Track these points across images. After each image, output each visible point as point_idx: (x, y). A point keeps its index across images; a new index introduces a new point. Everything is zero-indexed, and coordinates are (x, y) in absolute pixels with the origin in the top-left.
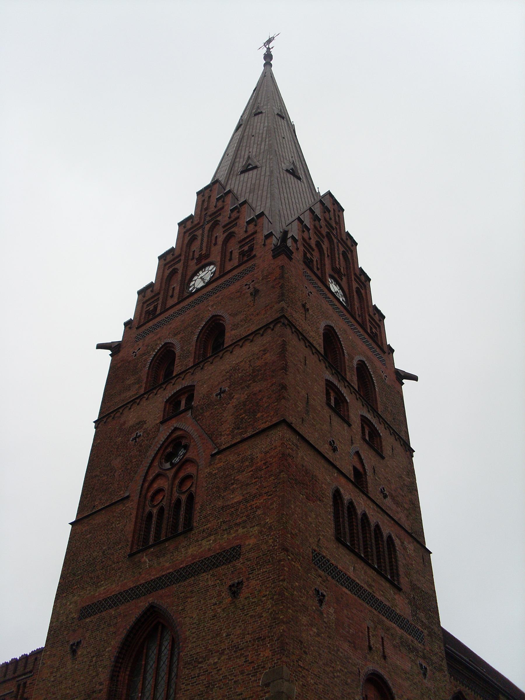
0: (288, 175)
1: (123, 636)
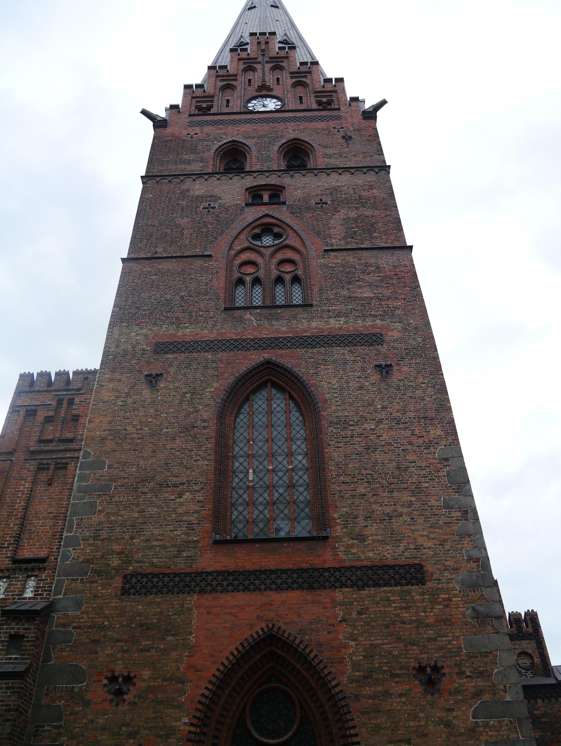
1: (231, 381)
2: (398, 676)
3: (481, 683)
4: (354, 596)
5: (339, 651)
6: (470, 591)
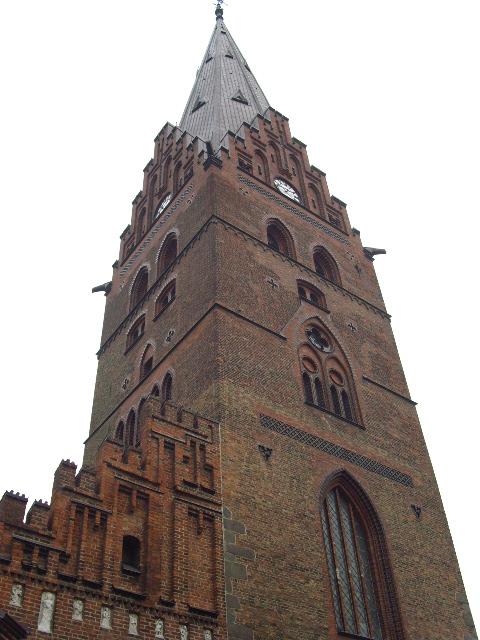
0: (235, 102)
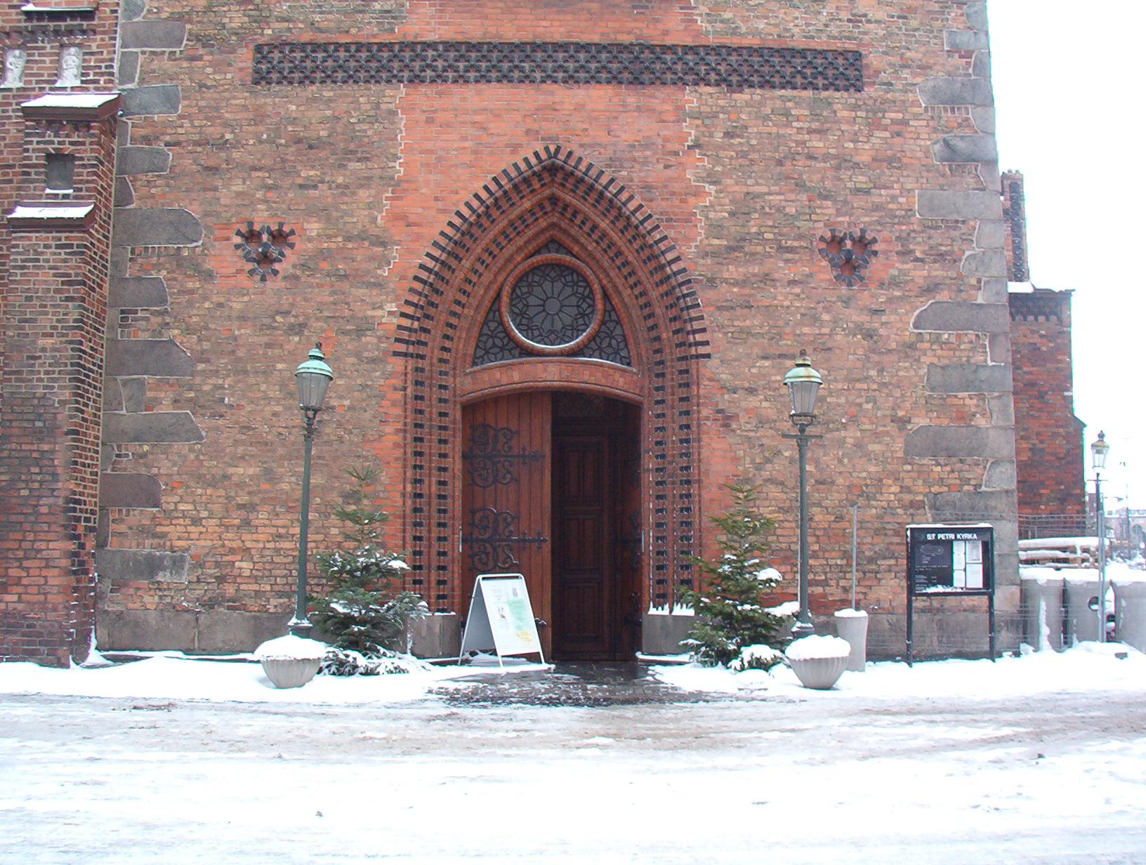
2: (790, 250)
3: (938, 272)
4: (721, 102)
5: (683, 201)
6: (946, 110)
